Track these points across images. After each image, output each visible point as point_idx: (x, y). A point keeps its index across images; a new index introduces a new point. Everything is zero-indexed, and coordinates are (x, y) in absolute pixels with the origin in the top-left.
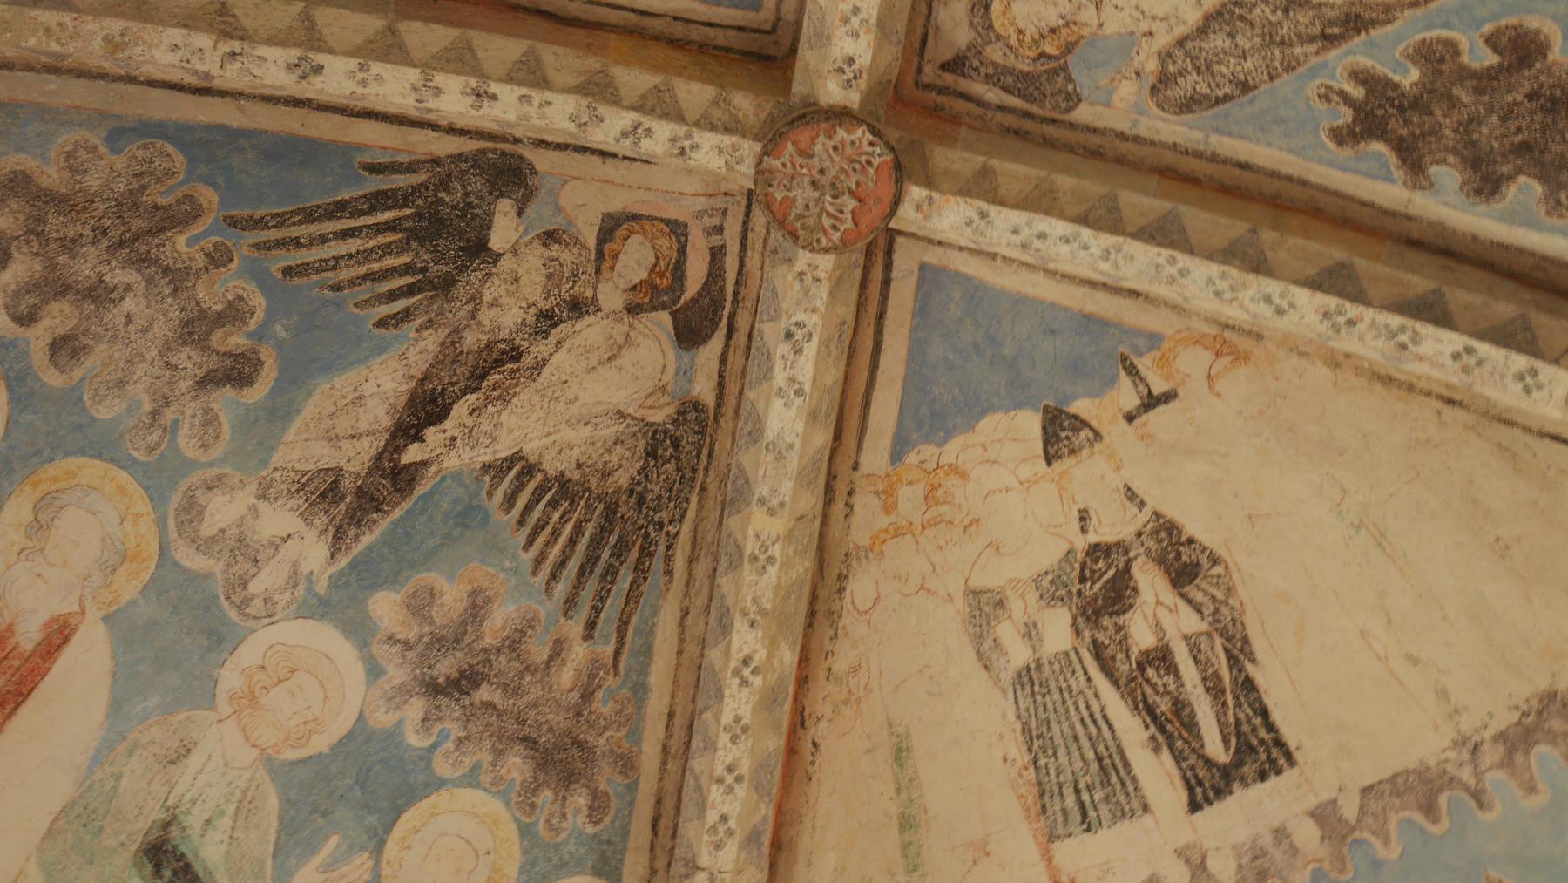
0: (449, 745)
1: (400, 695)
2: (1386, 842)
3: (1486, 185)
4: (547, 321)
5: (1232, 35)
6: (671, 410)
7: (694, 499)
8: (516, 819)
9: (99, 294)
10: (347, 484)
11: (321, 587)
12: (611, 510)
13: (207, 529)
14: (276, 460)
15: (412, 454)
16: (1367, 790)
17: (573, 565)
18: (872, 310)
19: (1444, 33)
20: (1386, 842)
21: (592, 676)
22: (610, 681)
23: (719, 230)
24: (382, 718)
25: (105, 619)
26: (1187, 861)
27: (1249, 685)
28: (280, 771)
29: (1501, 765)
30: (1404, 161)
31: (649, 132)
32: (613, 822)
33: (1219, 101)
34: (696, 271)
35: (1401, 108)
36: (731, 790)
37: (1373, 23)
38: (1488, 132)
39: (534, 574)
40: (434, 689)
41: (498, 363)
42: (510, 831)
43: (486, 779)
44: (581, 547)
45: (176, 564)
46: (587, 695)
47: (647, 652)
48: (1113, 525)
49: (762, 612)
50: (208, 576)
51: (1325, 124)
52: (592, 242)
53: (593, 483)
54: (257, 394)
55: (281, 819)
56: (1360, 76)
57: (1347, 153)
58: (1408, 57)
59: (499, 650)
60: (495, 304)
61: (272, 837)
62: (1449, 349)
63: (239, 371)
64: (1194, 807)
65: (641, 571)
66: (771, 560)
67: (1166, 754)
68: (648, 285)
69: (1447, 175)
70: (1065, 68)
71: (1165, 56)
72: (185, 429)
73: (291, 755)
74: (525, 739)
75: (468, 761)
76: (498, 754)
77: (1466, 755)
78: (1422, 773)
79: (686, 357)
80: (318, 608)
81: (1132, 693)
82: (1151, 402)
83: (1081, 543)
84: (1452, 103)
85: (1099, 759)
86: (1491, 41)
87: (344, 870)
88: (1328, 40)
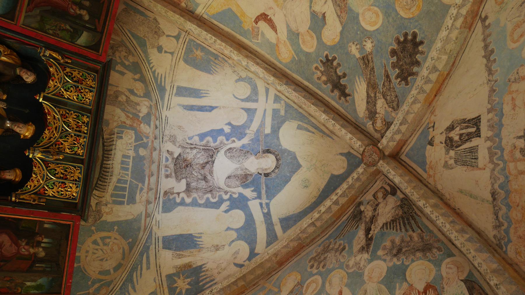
0: (405, 260)
1: (391, 260)
2: (495, 100)
3: (418, 63)
4: (375, 210)
5: (388, 95)
6: (400, 202)
7: (414, 207)
8: (427, 260)
9: (325, 258)
10: (364, 246)
11: (369, 258)
12: (403, 218)
13: (351, 266)
14: (354, 252)
15: (370, 236)
16: (488, 103)
17: (402, 226)
18: (407, 166)
19: (390, 63)
20: (495, 100)
21: (420, 236)
22: (424, 234)
23: (386, 182)
24: (391, 264)
25: (345, 286)
26: (487, 140)
27: (469, 120)
28: (381, 282)
29: (493, 76)
30: (412, 75)
31: (354, 177)
32: (444, 249)
33: (398, 101)
34: (388, 188)
35: (403, 73)
36: (439, 219)
37: (388, 74)
38: (408, 60)
39: (397, 231)
40: (395, 255)
41: (373, 219)
42: (427, 262)
43: (415, 259)
44: (402, 224)
45: (350, 273)
46: (422, 238)
47: (426, 227)
48: (443, 138)
49: (419, 198)
50: (355, 270)
51: (404, 86)
52: (373, 199)
53: (397, 217)
54: (347, 248)
55: (386, 288)
56: (397, 78)
57: (410, 84)
58: (394, 70)
59: (401, 244)
60: (367, 214)
61: (387, 291)
62: (426, 71)
63: (344, 249)
64: (480, 136)
65: (414, 219)
66: (413, 192)
67: (473, 139)
68: (384, 195)
69: (415, 69)
70: (387, 122)
71: (389, 107)
72: (341, 259)
73: (381, 279)
74: (417, 250)
75: (410, 259)
76: (414, 255)
77: (490, 83)
78: (490, 91)
79: (396, 196)
80: (370, 261)
81: (464, 143)
82: (433, 126)
83: (444, 145)
84: (402, 65)
85: (469, 152)
86: (392, 57)
87: (403, 287)
88: (390, 81)
